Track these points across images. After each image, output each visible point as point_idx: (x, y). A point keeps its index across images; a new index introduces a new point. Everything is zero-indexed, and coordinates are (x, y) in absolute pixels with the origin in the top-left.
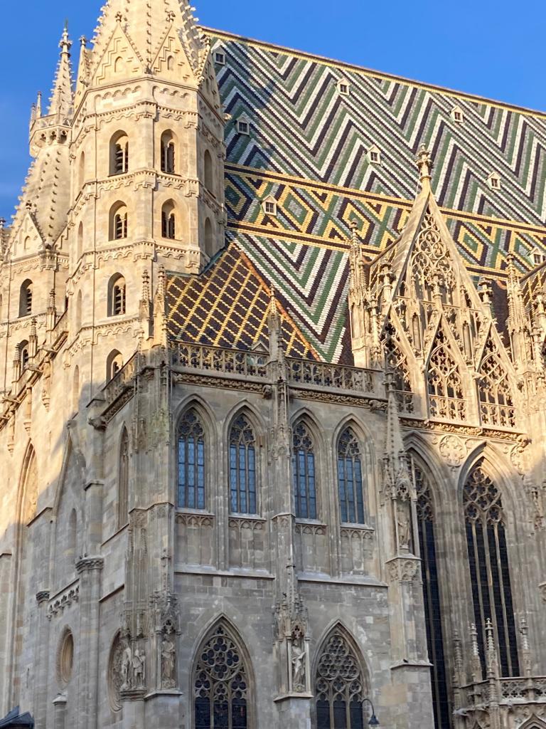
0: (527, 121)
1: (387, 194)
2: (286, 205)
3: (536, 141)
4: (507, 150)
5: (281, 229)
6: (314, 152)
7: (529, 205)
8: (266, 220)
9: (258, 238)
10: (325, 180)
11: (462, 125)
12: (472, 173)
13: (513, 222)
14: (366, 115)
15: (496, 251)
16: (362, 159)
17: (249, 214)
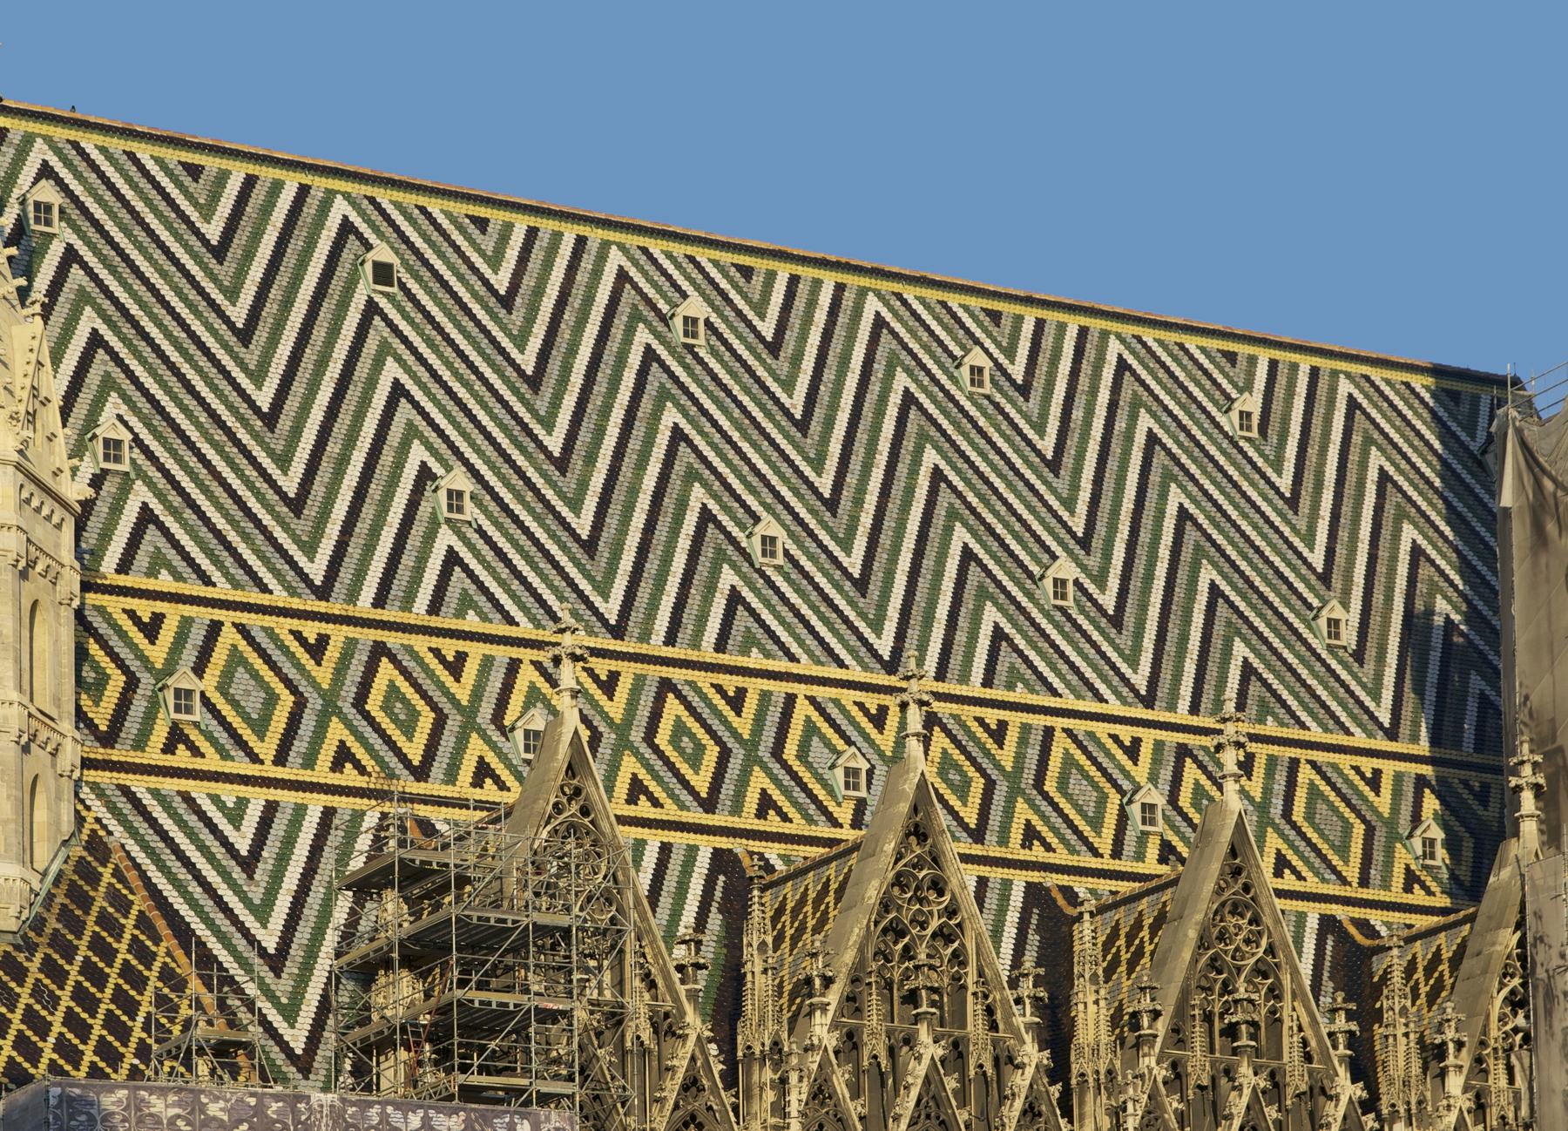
0: (885, 313)
1: (484, 618)
2: (223, 689)
3: (901, 381)
4: (815, 427)
5: (212, 762)
6: (297, 505)
7: (851, 603)
8: (176, 737)
9: (155, 793)
10: (323, 592)
11: (702, 353)
12: (714, 519)
13: (805, 667)
14: (440, 356)
15: (751, 760)
16: (424, 510)
17: (131, 726)
